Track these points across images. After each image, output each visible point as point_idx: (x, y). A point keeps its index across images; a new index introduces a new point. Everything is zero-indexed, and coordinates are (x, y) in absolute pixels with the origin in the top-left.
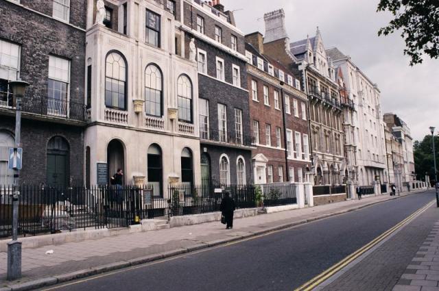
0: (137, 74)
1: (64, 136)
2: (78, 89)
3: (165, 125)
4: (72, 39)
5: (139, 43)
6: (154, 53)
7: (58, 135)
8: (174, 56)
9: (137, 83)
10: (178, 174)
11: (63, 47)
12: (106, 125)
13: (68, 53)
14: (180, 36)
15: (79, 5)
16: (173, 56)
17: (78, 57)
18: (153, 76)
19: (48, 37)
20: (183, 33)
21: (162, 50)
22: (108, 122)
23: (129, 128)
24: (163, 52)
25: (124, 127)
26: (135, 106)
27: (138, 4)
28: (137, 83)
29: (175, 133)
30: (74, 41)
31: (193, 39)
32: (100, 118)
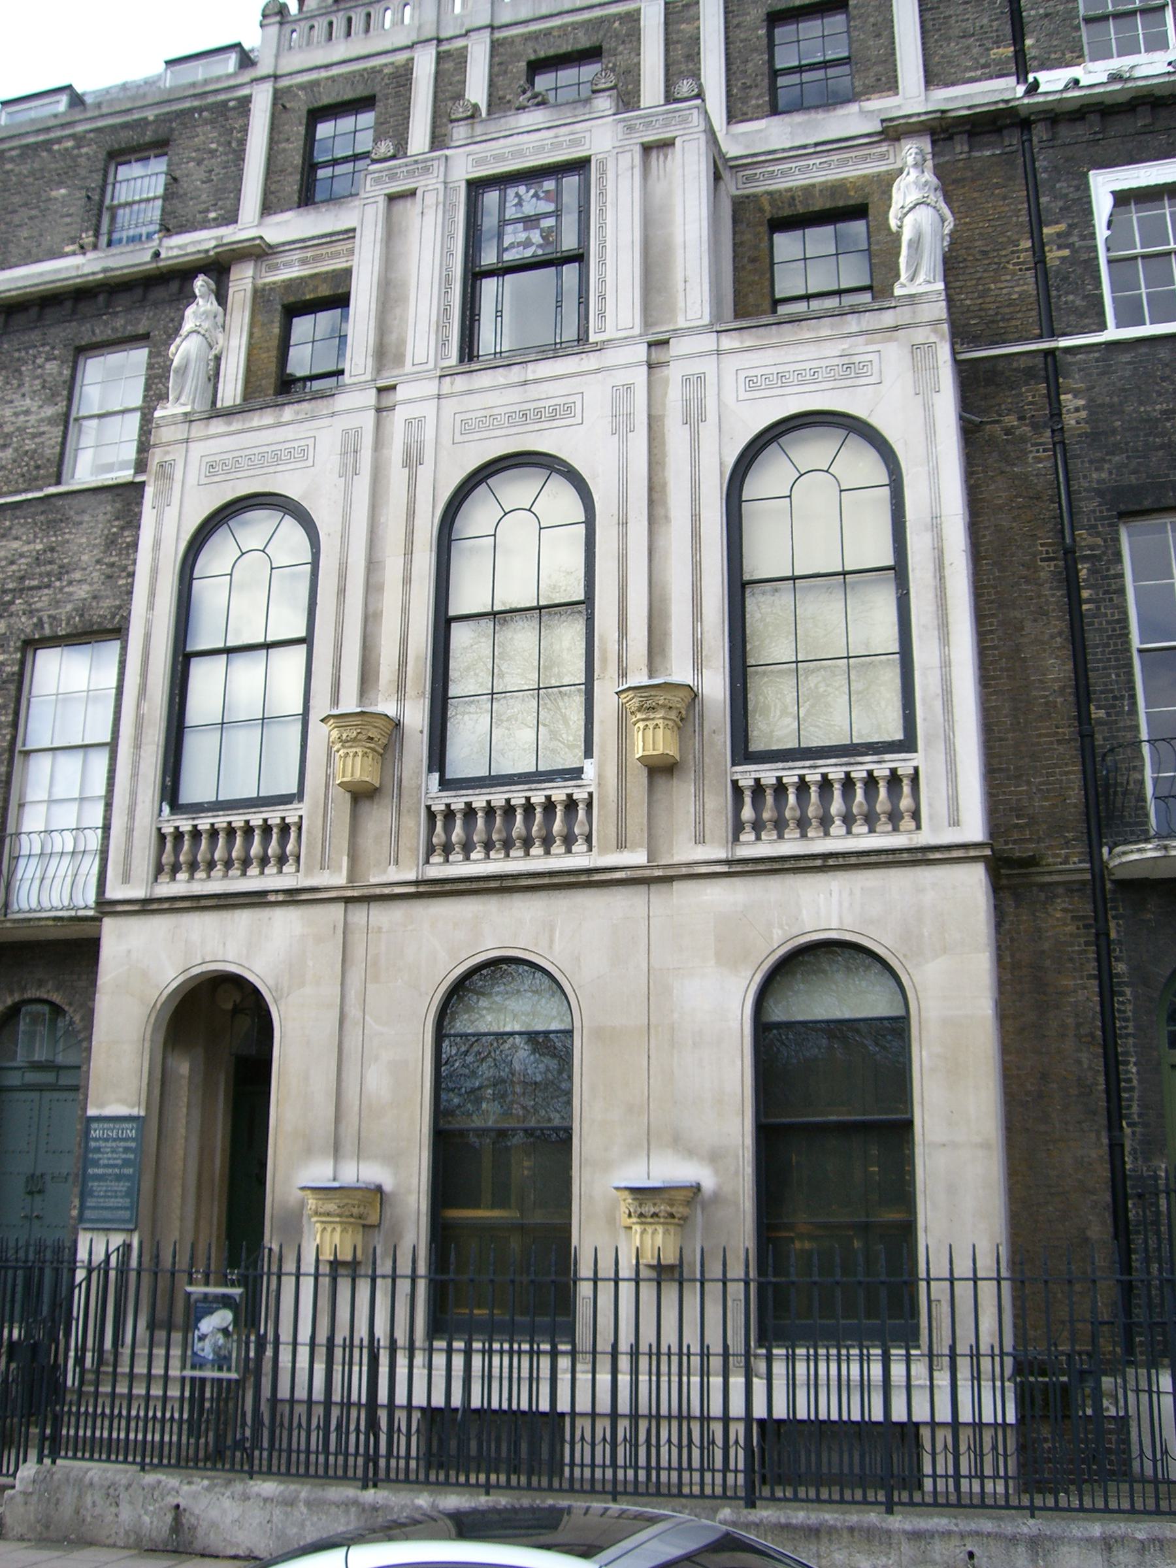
0: (373, 565)
1: (56, 998)
3: (603, 823)
6: (514, 395)
7: (28, 995)
9: (370, 619)
10: (714, 1157)
11: (82, 592)
12: (146, 907)
19: (22, 578)
22: (180, 886)
23: (293, 897)
25: (257, 900)
27: (413, 193)
28: (370, 619)
29: (686, 851)
32: (126, 878)
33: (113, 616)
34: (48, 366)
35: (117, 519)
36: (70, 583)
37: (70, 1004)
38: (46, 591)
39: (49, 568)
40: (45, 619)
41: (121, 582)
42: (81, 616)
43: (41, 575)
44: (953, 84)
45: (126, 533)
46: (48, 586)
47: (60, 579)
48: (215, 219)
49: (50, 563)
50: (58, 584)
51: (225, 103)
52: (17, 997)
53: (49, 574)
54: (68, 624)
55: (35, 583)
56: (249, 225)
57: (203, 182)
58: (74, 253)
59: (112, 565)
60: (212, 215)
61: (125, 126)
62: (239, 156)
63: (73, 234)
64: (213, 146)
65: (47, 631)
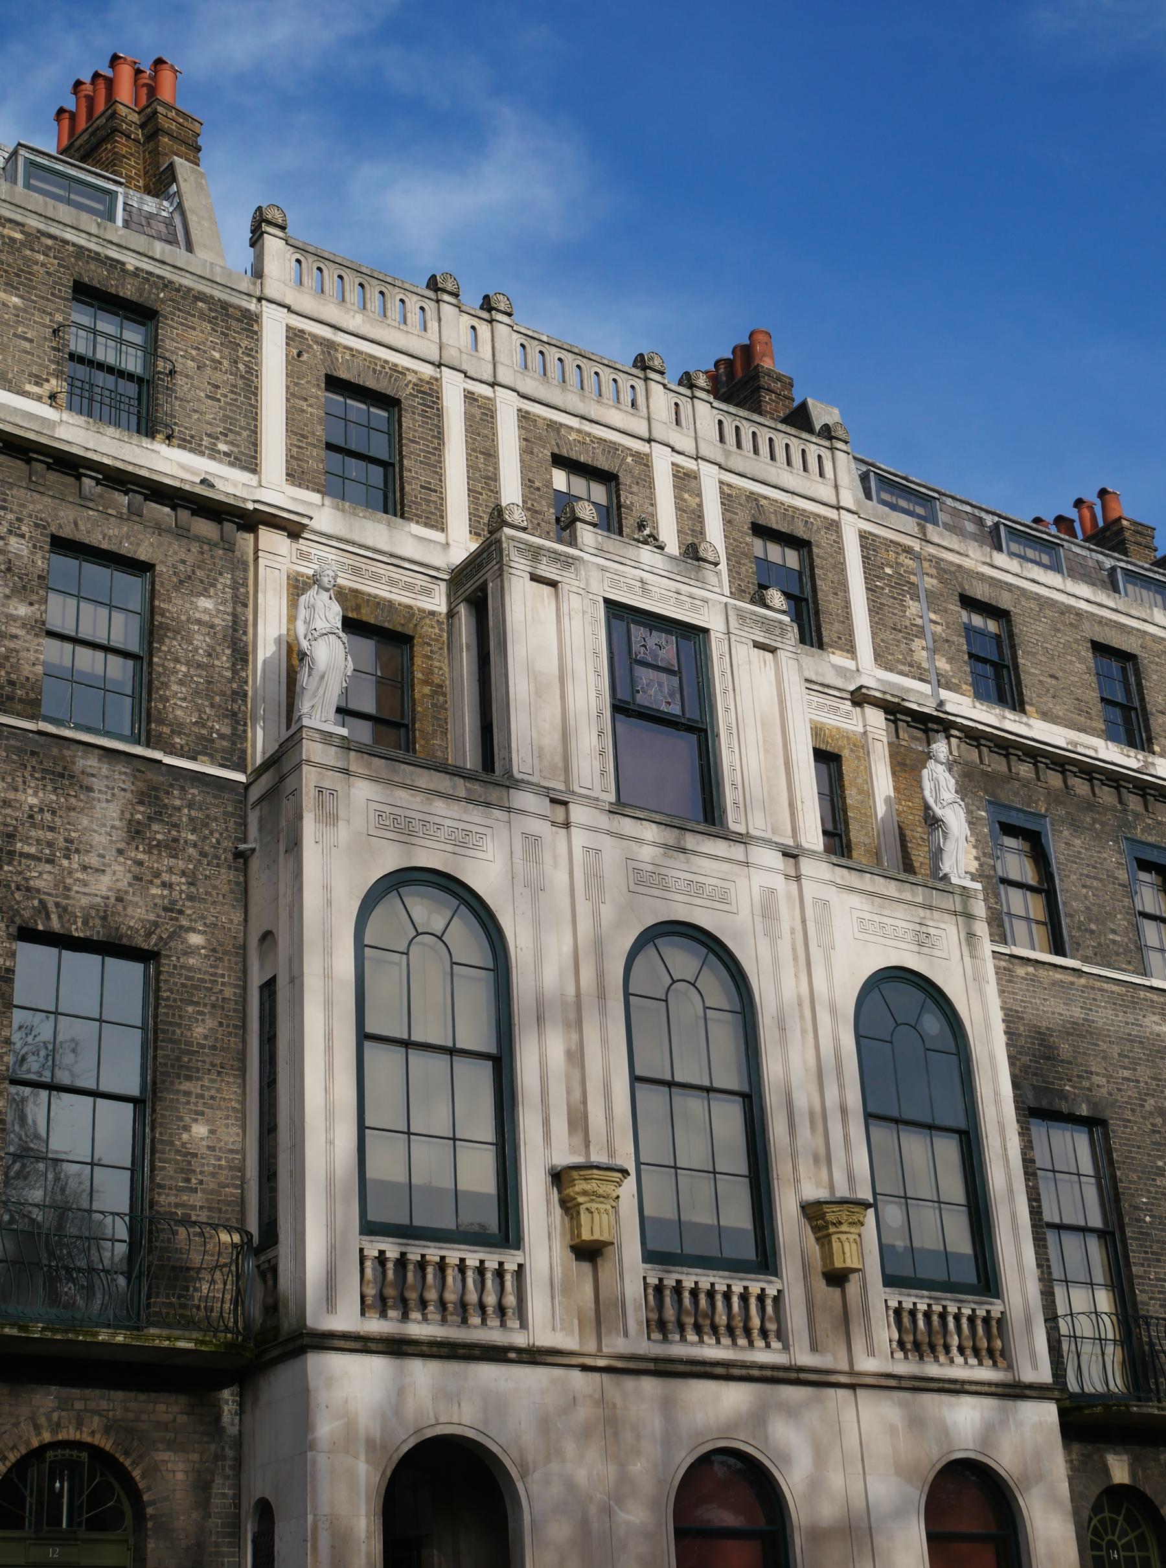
2: (200, 1130)
4: (159, 831)
5: (578, 813)
8: (819, 872)
11: (103, 885)
13: (137, 916)
14: (862, 745)
15: (201, 641)
16: (807, 866)
17: (195, 939)
18: (687, 1006)
20: (876, 718)
21: (743, 839)
24: (737, 852)
26: (569, 1206)
30: (172, 847)
31: (941, 748)
33: (149, 934)
34: (13, 540)
35: (141, 802)
36: (85, 868)
37: (127, 1453)
38: (48, 867)
39: (50, 836)
40: (52, 907)
41: (155, 891)
42: (104, 918)
43: (38, 841)
44: (891, 671)
45: (156, 827)
46: (50, 861)
47: (68, 857)
48: (225, 454)
49: (52, 829)
50: (65, 863)
51: (225, 306)
52: (47, 1437)
53: (50, 844)
54: (85, 923)
55: (33, 850)
56: (271, 486)
57: (208, 397)
58: (39, 399)
59: (140, 863)
60: (222, 447)
61: (96, 257)
62: (250, 386)
63: (35, 369)
64: (217, 355)
65: (55, 925)
